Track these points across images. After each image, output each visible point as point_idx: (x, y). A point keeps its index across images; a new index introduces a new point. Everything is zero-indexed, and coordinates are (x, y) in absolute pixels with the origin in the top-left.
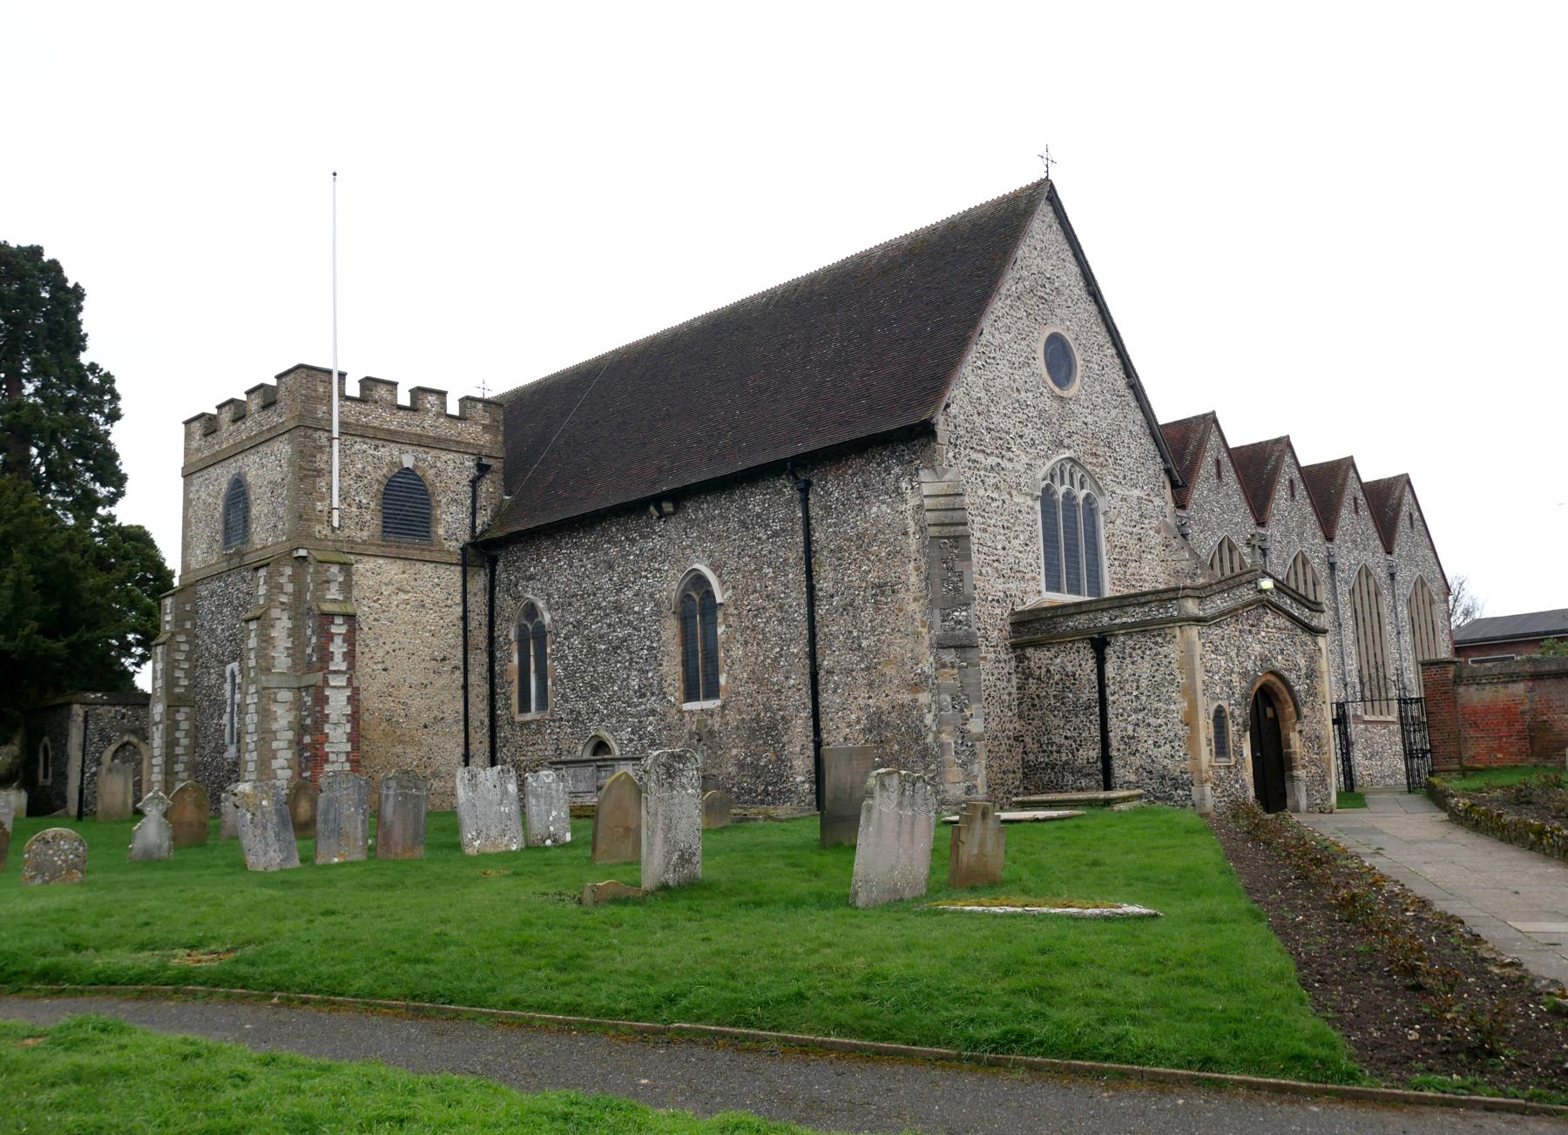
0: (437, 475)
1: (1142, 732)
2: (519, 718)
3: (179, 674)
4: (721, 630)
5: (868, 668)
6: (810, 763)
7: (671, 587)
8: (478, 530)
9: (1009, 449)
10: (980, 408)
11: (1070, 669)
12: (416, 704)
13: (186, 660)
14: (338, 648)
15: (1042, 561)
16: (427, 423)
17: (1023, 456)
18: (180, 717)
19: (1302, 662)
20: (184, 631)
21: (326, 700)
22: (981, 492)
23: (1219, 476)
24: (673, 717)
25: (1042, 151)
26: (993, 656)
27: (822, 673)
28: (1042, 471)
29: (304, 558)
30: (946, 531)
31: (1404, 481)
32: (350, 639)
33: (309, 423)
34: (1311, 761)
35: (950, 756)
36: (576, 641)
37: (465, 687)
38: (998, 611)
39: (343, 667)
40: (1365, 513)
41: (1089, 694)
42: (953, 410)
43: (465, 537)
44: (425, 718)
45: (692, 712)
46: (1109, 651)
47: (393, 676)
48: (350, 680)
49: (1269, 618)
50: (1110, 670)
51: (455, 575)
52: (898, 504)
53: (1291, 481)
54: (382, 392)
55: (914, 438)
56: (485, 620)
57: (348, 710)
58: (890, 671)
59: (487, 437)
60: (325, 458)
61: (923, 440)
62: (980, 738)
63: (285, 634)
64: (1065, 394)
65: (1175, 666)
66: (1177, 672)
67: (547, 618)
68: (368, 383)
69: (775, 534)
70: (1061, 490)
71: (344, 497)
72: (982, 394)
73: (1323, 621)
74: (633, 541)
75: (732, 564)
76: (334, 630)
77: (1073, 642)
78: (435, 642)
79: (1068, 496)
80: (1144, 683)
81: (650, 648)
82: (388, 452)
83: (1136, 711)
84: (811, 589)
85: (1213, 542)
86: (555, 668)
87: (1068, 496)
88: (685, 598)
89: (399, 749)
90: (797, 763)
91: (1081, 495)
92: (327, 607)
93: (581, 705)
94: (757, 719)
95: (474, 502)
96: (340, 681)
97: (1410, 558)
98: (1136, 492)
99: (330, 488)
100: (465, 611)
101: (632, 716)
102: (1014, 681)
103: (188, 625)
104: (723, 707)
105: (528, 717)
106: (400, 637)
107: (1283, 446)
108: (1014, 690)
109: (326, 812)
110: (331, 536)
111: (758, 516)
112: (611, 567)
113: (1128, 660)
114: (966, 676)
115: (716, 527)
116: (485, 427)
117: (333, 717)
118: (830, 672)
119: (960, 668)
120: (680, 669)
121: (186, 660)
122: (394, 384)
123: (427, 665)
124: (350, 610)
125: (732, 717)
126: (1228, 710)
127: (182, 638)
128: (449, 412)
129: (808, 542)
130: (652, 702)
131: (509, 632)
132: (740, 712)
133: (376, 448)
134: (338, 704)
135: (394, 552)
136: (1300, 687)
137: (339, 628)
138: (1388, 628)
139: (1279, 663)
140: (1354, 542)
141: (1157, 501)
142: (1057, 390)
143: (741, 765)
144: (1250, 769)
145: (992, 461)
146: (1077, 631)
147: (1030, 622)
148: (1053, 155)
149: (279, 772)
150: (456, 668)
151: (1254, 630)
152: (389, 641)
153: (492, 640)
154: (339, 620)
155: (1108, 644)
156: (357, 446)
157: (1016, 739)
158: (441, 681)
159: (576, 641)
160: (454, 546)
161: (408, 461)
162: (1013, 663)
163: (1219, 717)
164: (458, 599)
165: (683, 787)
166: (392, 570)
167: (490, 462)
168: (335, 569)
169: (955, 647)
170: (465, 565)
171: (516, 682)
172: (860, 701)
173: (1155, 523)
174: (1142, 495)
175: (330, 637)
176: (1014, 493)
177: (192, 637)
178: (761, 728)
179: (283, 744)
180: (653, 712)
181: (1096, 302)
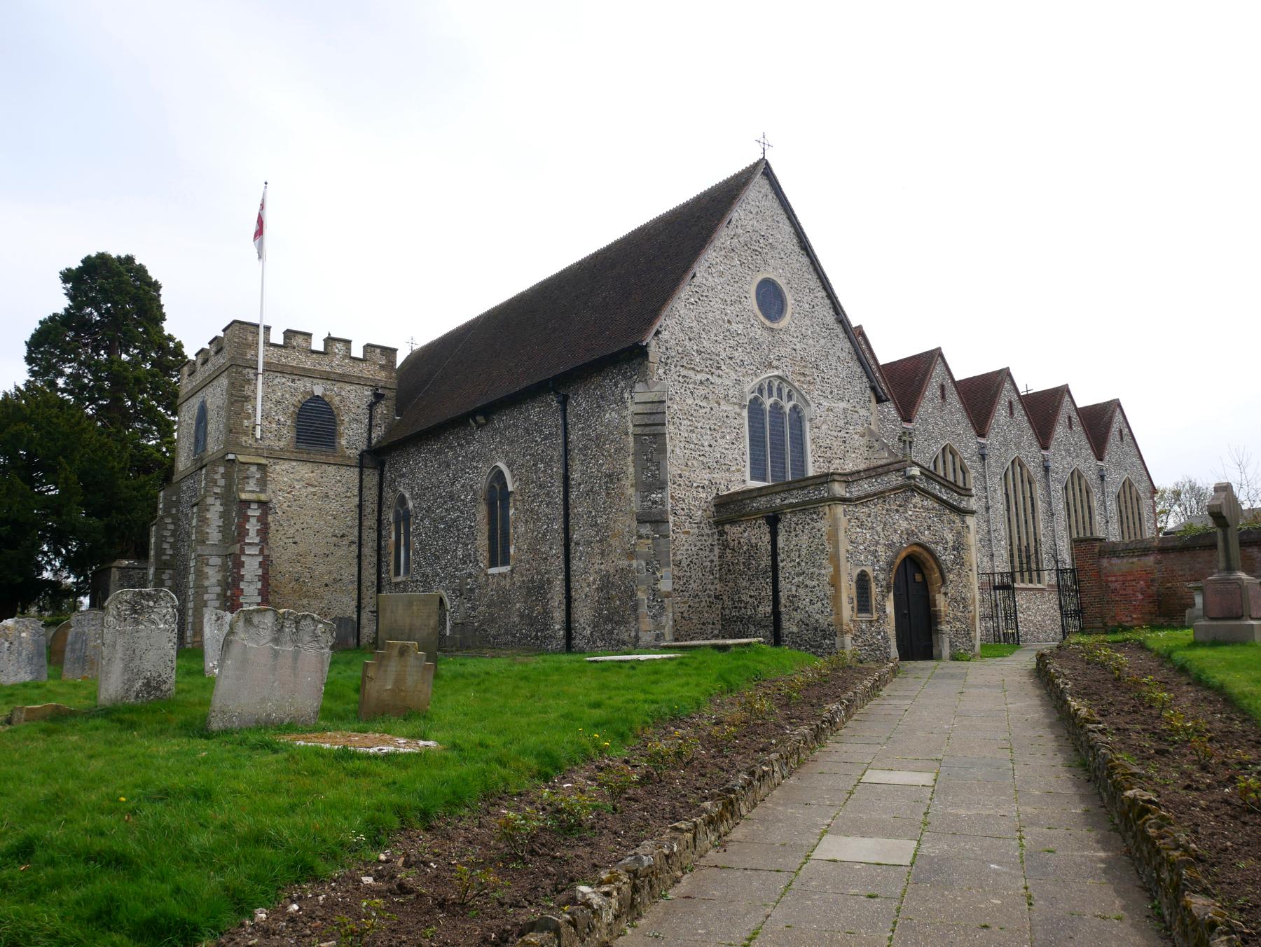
0: (341, 401)
1: (802, 592)
2: (394, 580)
3: (166, 546)
4: (512, 512)
5: (601, 541)
6: (563, 614)
7: (482, 483)
8: (374, 441)
9: (719, 368)
10: (692, 336)
11: (754, 541)
12: (321, 568)
14: (252, 527)
15: (747, 458)
16: (336, 364)
17: (732, 373)
18: (165, 577)
19: (950, 537)
21: (242, 564)
22: (689, 401)
23: (943, 397)
25: (760, 137)
26: (696, 531)
27: (573, 544)
28: (750, 385)
29: (233, 460)
30: (647, 430)
31: (1115, 405)
32: (263, 520)
33: (239, 362)
34: (956, 619)
35: (643, 610)
36: (427, 522)
37: (359, 557)
38: (704, 495)
39: (257, 540)
40: (1078, 428)
41: (766, 562)
42: (665, 335)
43: (363, 446)
44: (326, 579)
46: (780, 526)
47: (301, 548)
48: (261, 550)
49: (917, 499)
50: (781, 542)
51: (352, 475)
52: (622, 409)
53: (1010, 403)
54: (300, 340)
55: (632, 357)
56: (375, 507)
57: (260, 572)
58: (615, 542)
59: (383, 374)
60: (252, 388)
61: (640, 360)
62: (668, 595)
63: (217, 515)
64: (775, 326)
65: (825, 538)
66: (826, 543)
67: (411, 504)
68: (289, 334)
69: (545, 439)
70: (768, 402)
71: (265, 416)
72: (694, 324)
73: (973, 504)
74: (461, 446)
75: (520, 461)
76: (250, 513)
77: (756, 519)
78: (336, 523)
79: (776, 407)
80: (804, 552)
81: (471, 527)
82: (303, 385)
83: (798, 575)
84: (566, 479)
85: (936, 449)
86: (415, 543)
87: (776, 407)
88: (491, 487)
90: (556, 614)
91: (788, 406)
92: (244, 496)
94: (532, 581)
95: (370, 421)
96: (255, 551)
97: (1119, 464)
98: (843, 405)
99: (255, 409)
100: (361, 500)
102: (717, 551)
103: (174, 511)
104: (512, 571)
106: (308, 519)
107: (1003, 376)
108: (716, 559)
109: (73, 643)
110: (255, 445)
111: (536, 424)
112: (448, 466)
113: (793, 534)
114: (658, 545)
115: (510, 433)
116: (382, 367)
117: (248, 577)
118: (577, 544)
119: (654, 539)
120: (487, 542)
122: (310, 335)
123: (329, 540)
124: (263, 497)
125: (517, 578)
126: (871, 575)
128: (353, 355)
129: (566, 443)
130: (470, 568)
131: (390, 516)
132: (522, 575)
133: (293, 381)
134: (251, 567)
135: (305, 456)
136: (947, 557)
137: (254, 512)
138: (1097, 517)
139: (926, 537)
140: (1068, 451)
141: (863, 412)
142: (767, 323)
143: (522, 616)
144: (893, 623)
145: (699, 377)
146: (758, 510)
147: (728, 504)
148: (769, 139)
150: (353, 542)
151: (901, 510)
152: (298, 522)
153: (379, 521)
154: (254, 506)
155: (780, 520)
156: (278, 380)
157: (716, 597)
158: (340, 552)
159: (427, 522)
160: (354, 453)
161: (318, 391)
162: (716, 537)
163: (863, 582)
164: (356, 492)
165: (153, 622)
166: (303, 471)
167: (386, 392)
168: (253, 469)
169: (650, 522)
170: (361, 467)
172: (597, 567)
173: (860, 429)
174: (849, 406)
175: (247, 518)
176: (722, 402)
177: (176, 521)
178: (534, 587)
179: (213, 596)
180: (470, 575)
181: (808, 255)
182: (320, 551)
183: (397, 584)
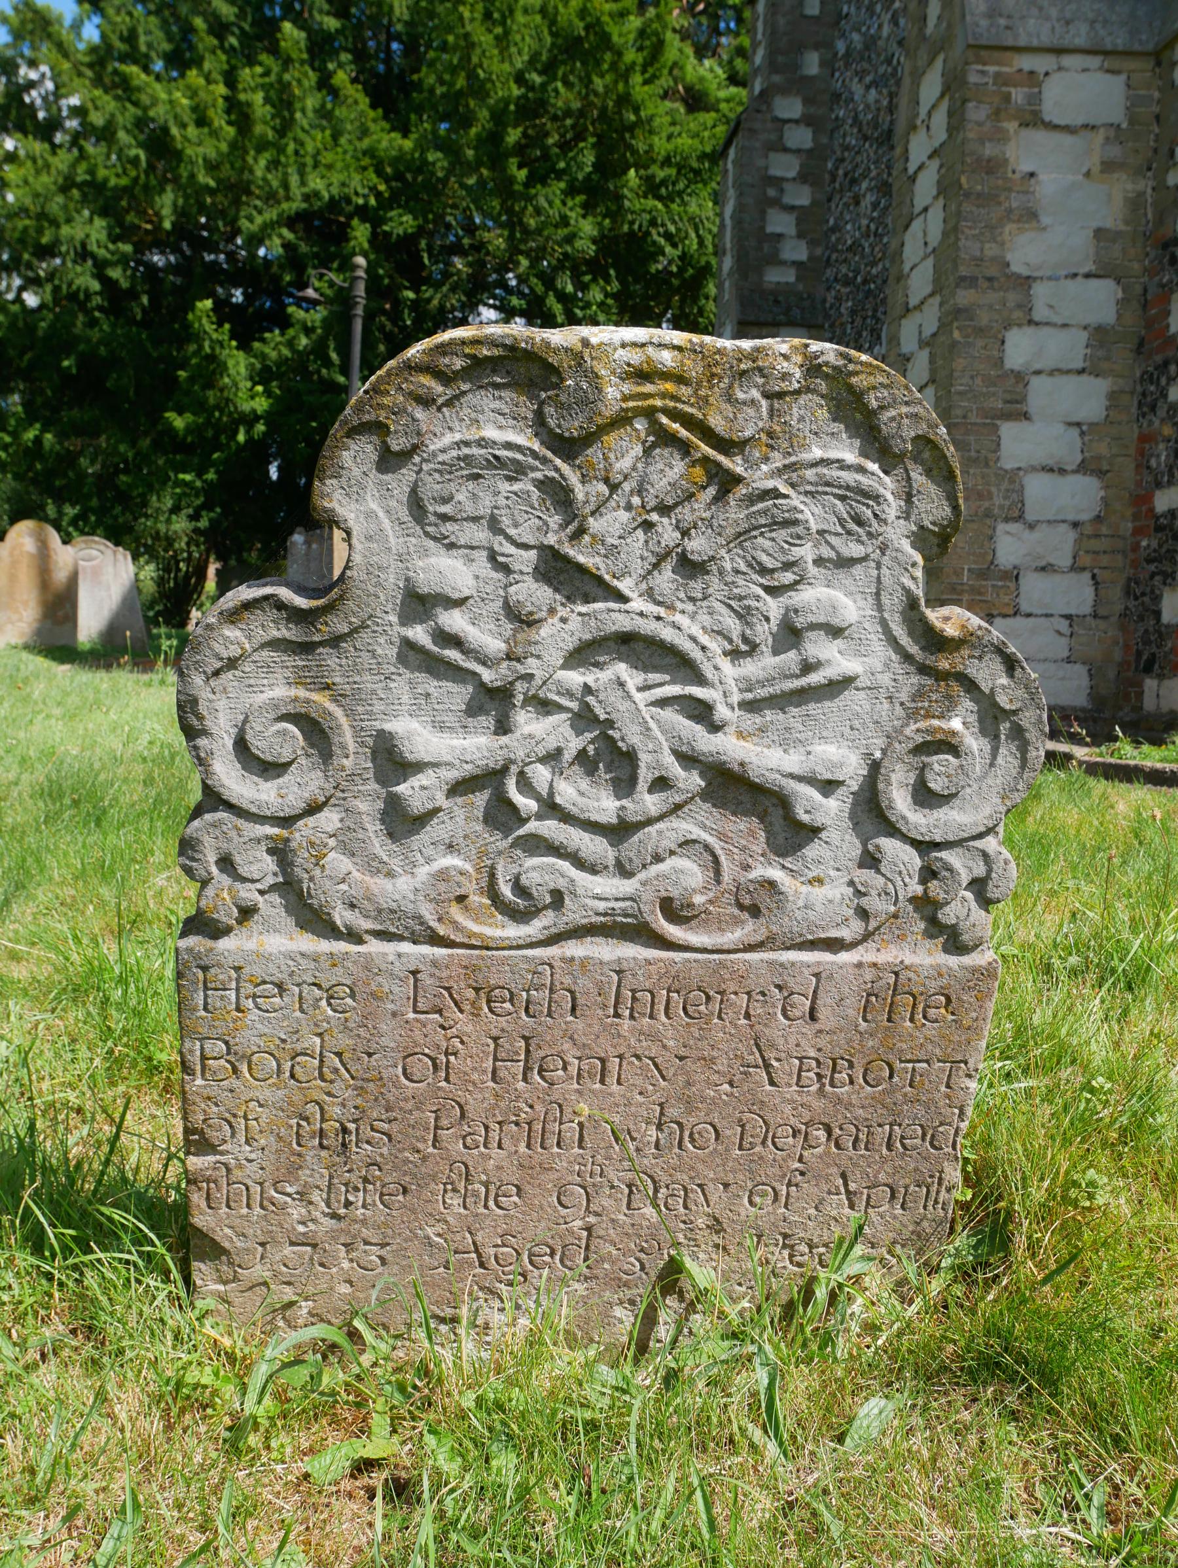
3: (780, 223)
13: (803, 177)
20: (798, 84)
103: (812, 64)
121: (803, 177)
127: (790, 107)
149: (1037, 488)
179: (1067, 347)
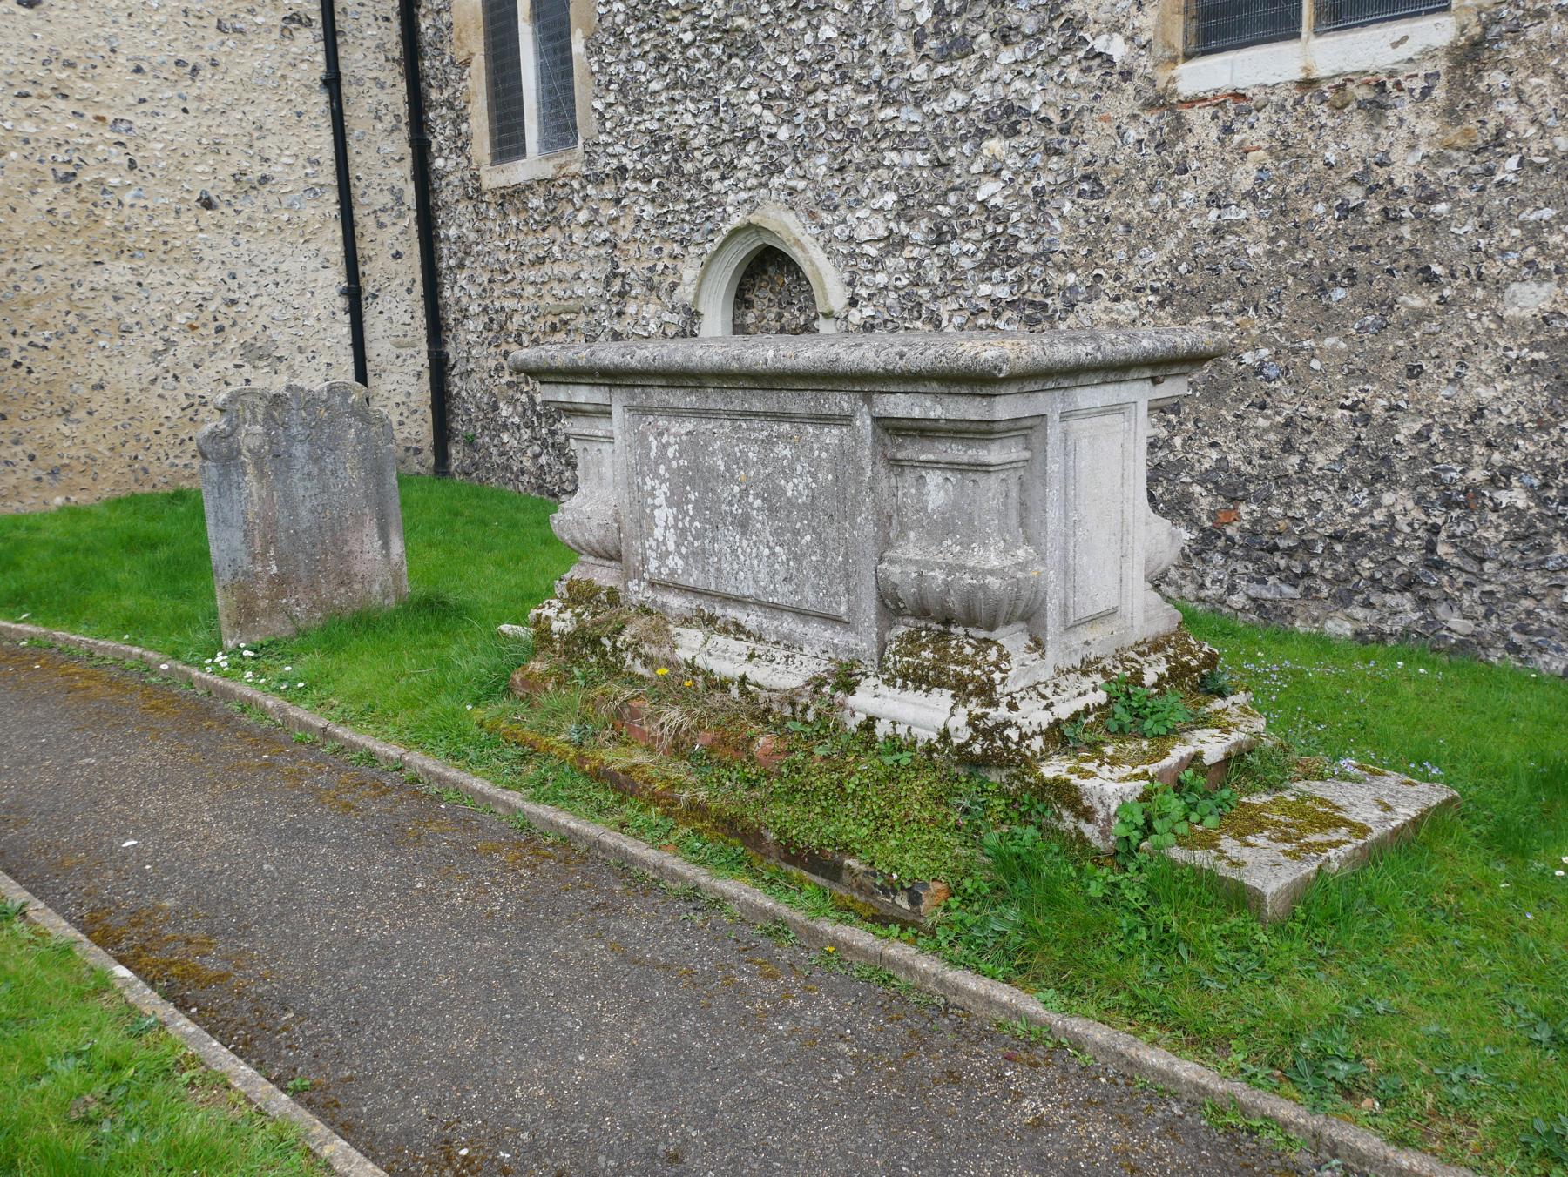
2: (496, 178)
12: (168, 131)
24: (1115, 128)
37: (333, 82)
44: (201, 175)
45: (1235, 104)
89: (118, 273)
93: (688, 119)
101: (902, 141)
105: (519, 172)
171: (479, 63)
182: (158, 48)
183: (512, 196)
